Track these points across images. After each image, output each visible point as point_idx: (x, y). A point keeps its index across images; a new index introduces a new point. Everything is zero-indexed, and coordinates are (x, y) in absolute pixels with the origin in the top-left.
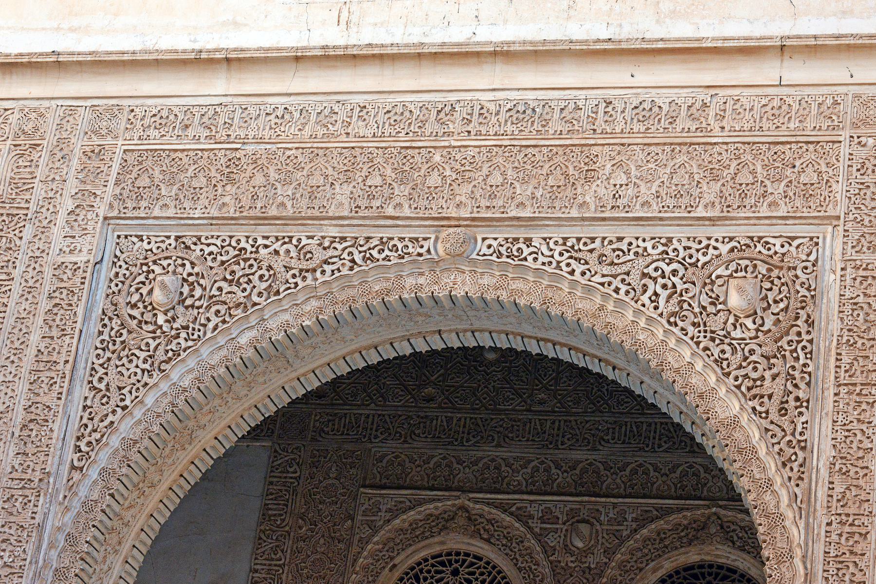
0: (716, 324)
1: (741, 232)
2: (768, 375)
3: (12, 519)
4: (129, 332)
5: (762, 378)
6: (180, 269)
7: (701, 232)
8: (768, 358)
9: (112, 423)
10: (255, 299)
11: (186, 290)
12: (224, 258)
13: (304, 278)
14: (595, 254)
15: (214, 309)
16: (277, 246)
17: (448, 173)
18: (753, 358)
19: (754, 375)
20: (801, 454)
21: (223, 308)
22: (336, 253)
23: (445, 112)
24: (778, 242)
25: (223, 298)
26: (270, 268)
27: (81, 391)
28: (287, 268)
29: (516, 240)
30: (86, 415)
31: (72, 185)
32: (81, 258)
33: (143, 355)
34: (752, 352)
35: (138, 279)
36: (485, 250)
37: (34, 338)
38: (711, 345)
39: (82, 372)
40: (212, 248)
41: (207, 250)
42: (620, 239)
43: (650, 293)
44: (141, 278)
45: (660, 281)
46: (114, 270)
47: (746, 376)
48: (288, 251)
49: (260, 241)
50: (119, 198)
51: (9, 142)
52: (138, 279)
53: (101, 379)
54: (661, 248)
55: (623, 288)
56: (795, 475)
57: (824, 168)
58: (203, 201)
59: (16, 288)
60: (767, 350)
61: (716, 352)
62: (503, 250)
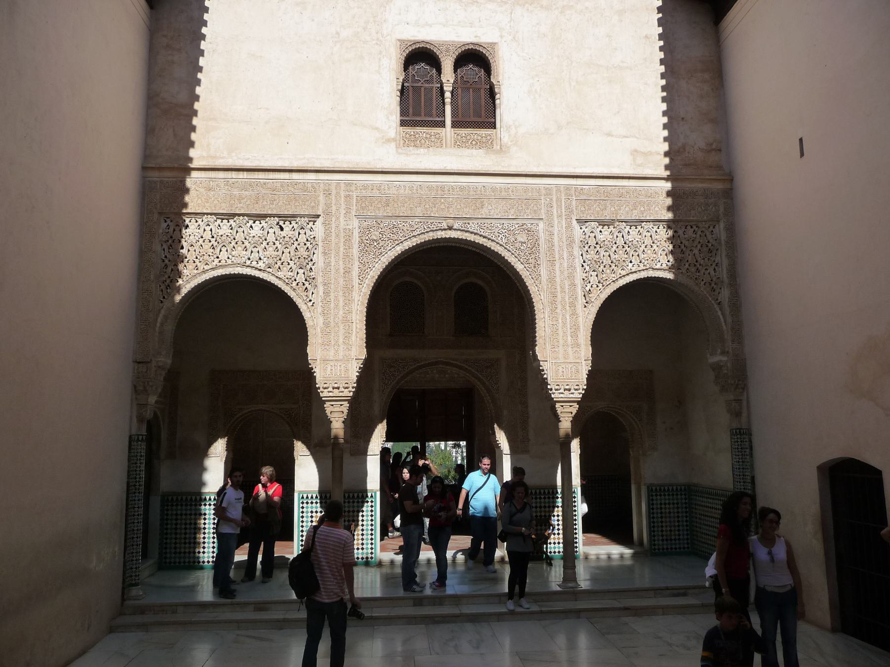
0: (517, 245)
1: (521, 222)
2: (530, 258)
3: (346, 298)
4: (367, 247)
5: (529, 259)
6: (378, 230)
7: (511, 222)
8: (530, 254)
9: (367, 272)
10: (400, 238)
11: (381, 235)
12: (390, 227)
13: (412, 233)
14: (486, 227)
15: (389, 241)
16: (404, 224)
17: (446, 205)
18: (526, 254)
19: (527, 258)
20: (540, 277)
21: (392, 241)
22: (420, 226)
23: (442, 188)
24: (529, 225)
25: (391, 238)
26: (403, 230)
27: (357, 264)
28: (408, 230)
29: (465, 223)
30: (360, 270)
31: (343, 206)
32: (351, 227)
33: (372, 254)
34: (526, 252)
35: (367, 233)
36: (458, 226)
37: (342, 249)
38: (516, 251)
39: (356, 259)
40: (386, 224)
41: (385, 225)
42: (491, 223)
43: (500, 237)
44: (368, 232)
45: (502, 234)
46: (359, 230)
47: (525, 259)
48: (407, 225)
49: (399, 223)
50: (357, 210)
51: (322, 193)
52: (367, 233)
53: (362, 260)
54: (502, 226)
55: (494, 236)
56: (539, 282)
57: (538, 206)
58: (381, 211)
59: (333, 235)
60: (529, 252)
61: (518, 252)
62: (462, 226)
